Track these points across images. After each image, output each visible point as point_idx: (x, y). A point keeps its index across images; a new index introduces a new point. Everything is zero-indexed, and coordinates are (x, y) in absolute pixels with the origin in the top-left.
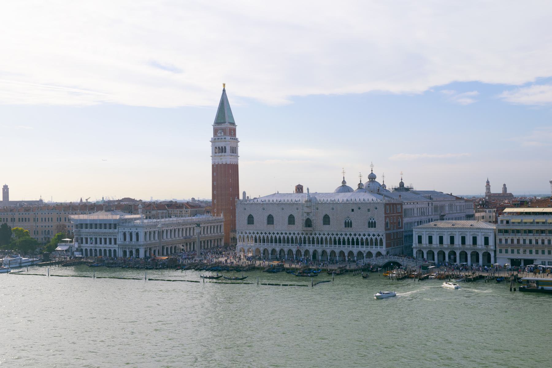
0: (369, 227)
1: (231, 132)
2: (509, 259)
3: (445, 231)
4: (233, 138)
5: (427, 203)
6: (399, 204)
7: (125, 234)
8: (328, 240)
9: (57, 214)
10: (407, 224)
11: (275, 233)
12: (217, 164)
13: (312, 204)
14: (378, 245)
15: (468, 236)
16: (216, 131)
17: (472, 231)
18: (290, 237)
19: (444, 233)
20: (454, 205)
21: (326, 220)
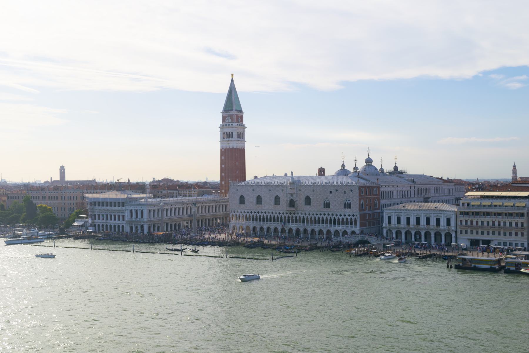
0: (345, 208)
1: (238, 119)
2: (468, 239)
3: (412, 212)
4: (240, 124)
5: (409, 186)
6: (375, 187)
7: (131, 211)
8: (309, 219)
9: (81, 192)
11: (263, 212)
12: (224, 148)
13: (295, 186)
14: (348, 225)
15: (432, 217)
16: (224, 118)
17: (435, 212)
18: (276, 216)
19: (411, 214)
20: (441, 188)
21: (308, 201)
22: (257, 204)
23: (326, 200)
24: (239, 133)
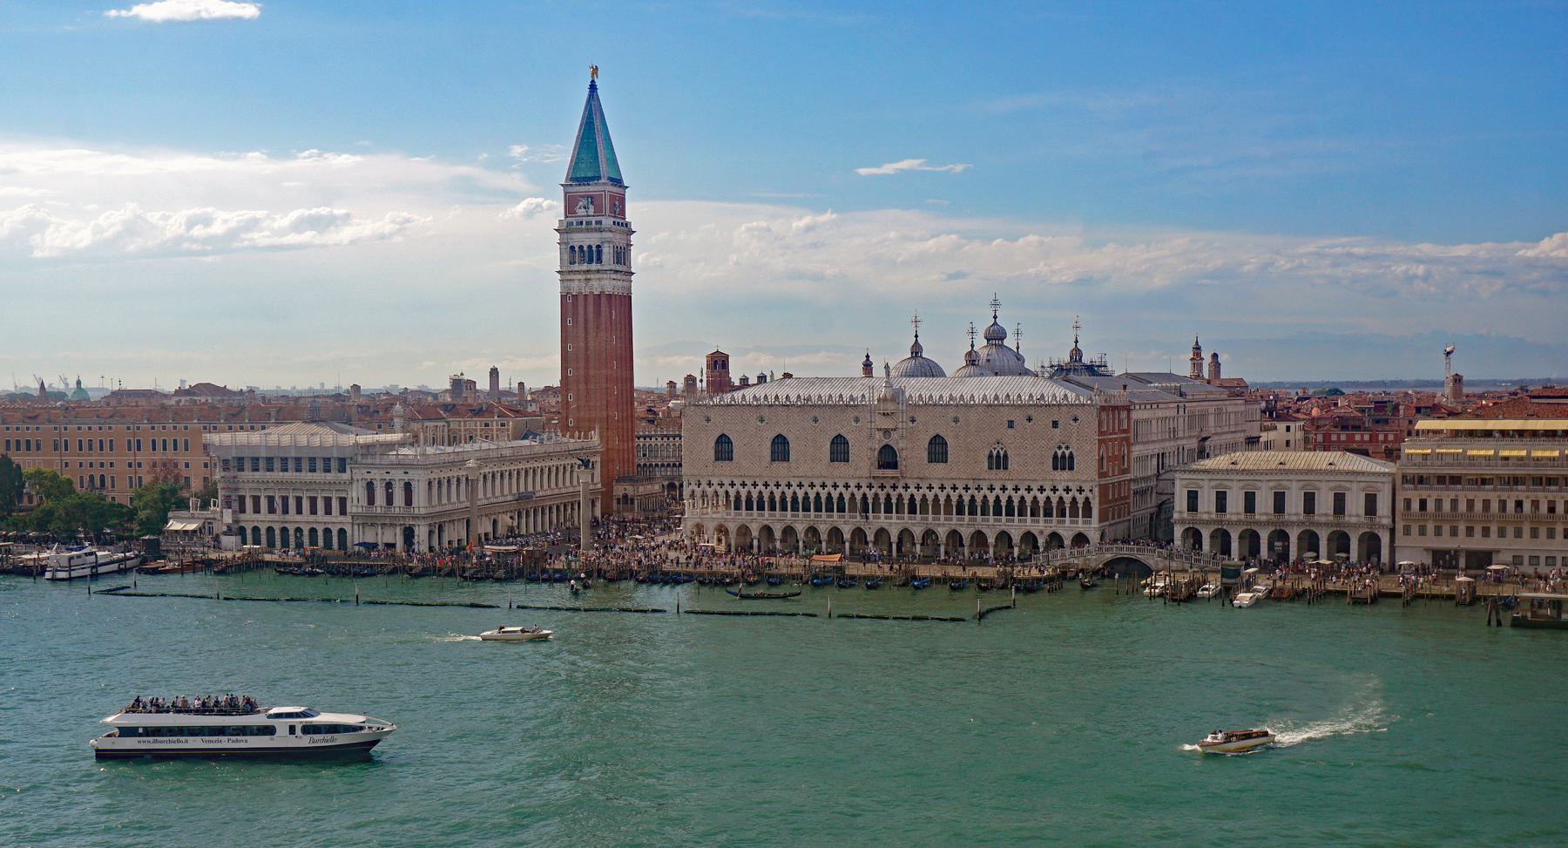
0: (1055, 468)
2: (1427, 550)
10: (1139, 459)
11: (792, 483)
16: (570, 205)
18: (835, 495)
19: (1259, 484)
21: (938, 450)
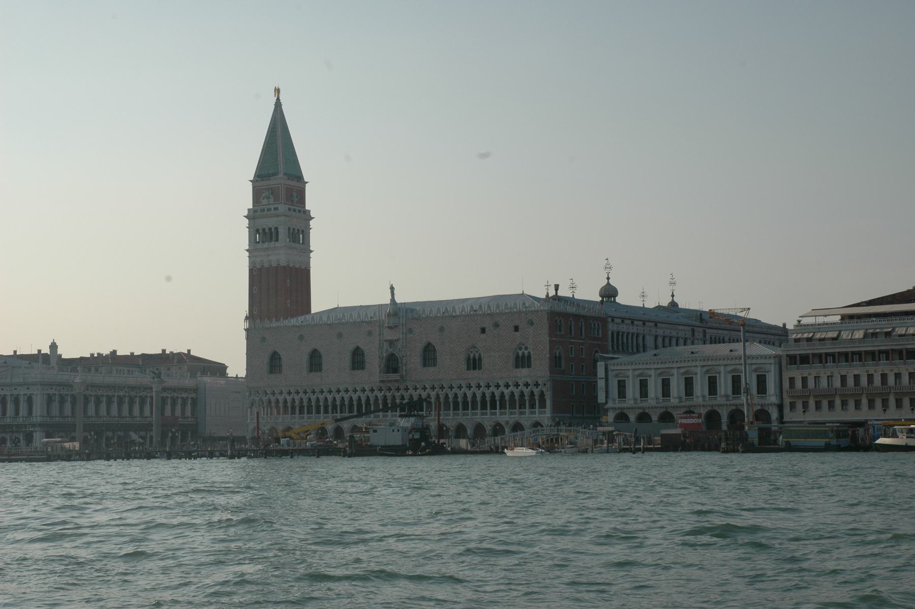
0: (517, 367)
1: (292, 195)
4: (297, 208)
12: (258, 267)
17: (729, 362)
18: (355, 397)
21: (429, 355)
22: (311, 371)
23: (472, 350)
24: (294, 229)
